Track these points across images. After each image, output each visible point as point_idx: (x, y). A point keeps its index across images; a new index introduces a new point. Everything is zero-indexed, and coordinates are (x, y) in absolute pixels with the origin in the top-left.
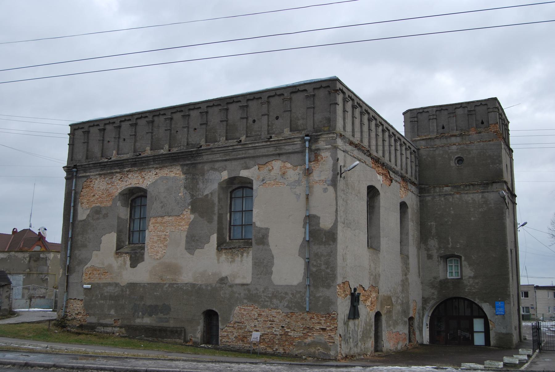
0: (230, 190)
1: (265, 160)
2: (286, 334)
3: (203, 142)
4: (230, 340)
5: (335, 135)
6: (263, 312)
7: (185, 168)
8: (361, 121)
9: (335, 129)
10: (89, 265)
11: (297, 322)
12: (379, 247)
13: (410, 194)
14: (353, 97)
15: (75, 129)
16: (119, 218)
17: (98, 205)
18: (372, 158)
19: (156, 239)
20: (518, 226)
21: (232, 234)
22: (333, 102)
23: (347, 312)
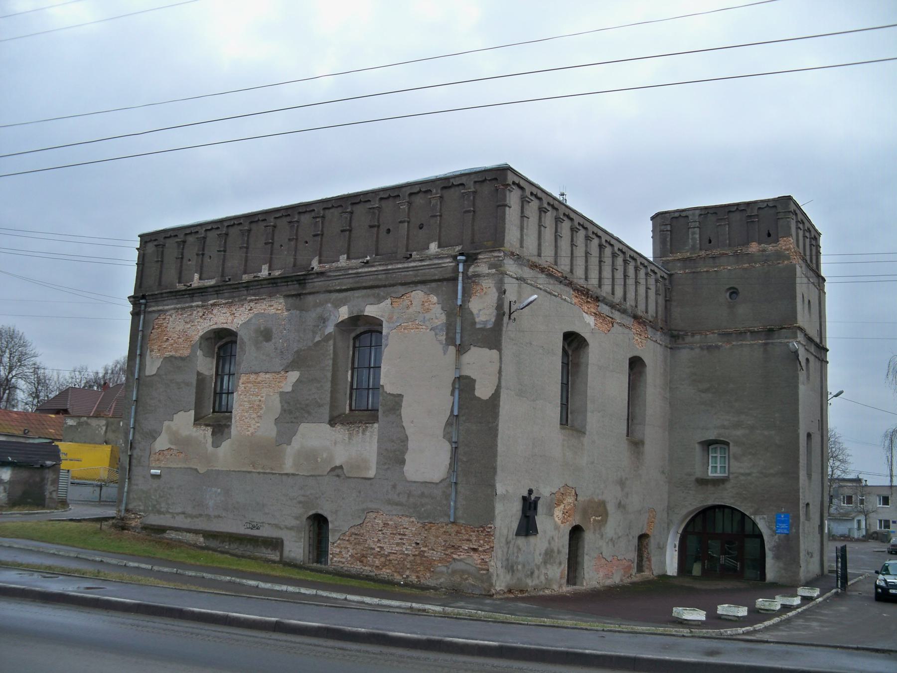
0: (353, 335)
1: (401, 290)
2: (421, 554)
3: (315, 264)
4: (343, 560)
5: (502, 254)
6: (391, 520)
7: (290, 300)
8: (556, 231)
9: (502, 245)
11: (437, 537)
12: (584, 427)
13: (651, 344)
14: (540, 194)
15: (146, 242)
16: (199, 374)
17: (173, 353)
18: (576, 289)
19: (247, 405)
20: (830, 397)
21: (353, 404)
22: (501, 203)
23: (515, 526)
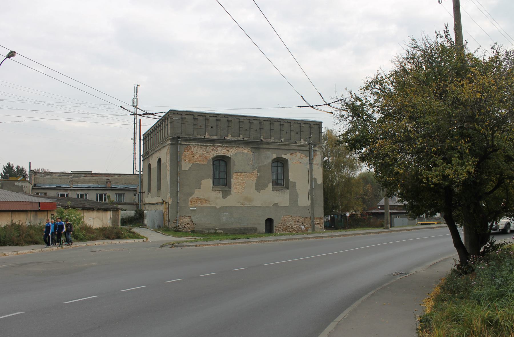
1: (293, 152)
3: (262, 138)
7: (253, 150)
10: (193, 196)
17: (197, 162)
